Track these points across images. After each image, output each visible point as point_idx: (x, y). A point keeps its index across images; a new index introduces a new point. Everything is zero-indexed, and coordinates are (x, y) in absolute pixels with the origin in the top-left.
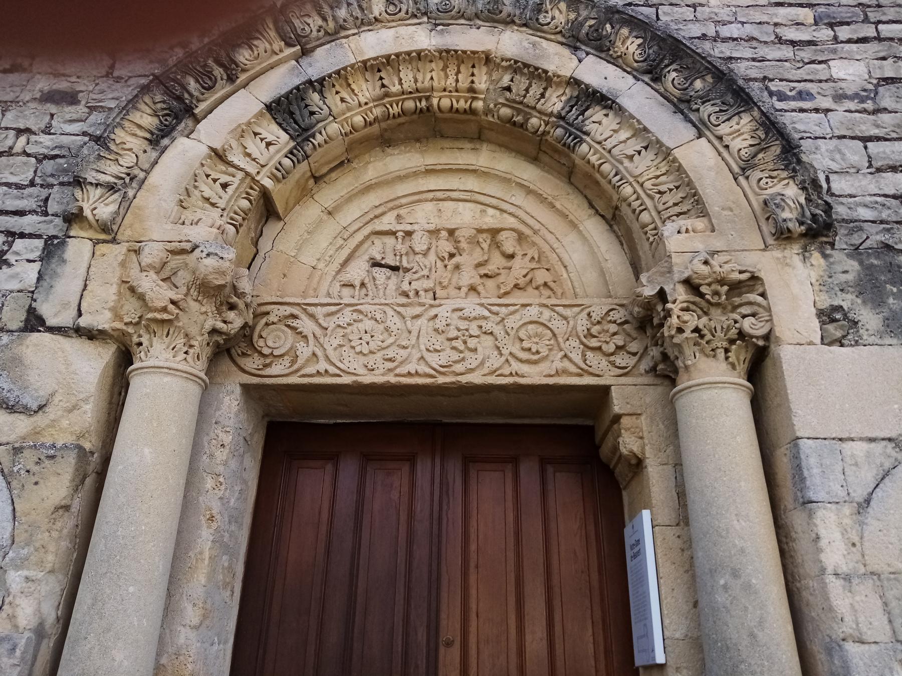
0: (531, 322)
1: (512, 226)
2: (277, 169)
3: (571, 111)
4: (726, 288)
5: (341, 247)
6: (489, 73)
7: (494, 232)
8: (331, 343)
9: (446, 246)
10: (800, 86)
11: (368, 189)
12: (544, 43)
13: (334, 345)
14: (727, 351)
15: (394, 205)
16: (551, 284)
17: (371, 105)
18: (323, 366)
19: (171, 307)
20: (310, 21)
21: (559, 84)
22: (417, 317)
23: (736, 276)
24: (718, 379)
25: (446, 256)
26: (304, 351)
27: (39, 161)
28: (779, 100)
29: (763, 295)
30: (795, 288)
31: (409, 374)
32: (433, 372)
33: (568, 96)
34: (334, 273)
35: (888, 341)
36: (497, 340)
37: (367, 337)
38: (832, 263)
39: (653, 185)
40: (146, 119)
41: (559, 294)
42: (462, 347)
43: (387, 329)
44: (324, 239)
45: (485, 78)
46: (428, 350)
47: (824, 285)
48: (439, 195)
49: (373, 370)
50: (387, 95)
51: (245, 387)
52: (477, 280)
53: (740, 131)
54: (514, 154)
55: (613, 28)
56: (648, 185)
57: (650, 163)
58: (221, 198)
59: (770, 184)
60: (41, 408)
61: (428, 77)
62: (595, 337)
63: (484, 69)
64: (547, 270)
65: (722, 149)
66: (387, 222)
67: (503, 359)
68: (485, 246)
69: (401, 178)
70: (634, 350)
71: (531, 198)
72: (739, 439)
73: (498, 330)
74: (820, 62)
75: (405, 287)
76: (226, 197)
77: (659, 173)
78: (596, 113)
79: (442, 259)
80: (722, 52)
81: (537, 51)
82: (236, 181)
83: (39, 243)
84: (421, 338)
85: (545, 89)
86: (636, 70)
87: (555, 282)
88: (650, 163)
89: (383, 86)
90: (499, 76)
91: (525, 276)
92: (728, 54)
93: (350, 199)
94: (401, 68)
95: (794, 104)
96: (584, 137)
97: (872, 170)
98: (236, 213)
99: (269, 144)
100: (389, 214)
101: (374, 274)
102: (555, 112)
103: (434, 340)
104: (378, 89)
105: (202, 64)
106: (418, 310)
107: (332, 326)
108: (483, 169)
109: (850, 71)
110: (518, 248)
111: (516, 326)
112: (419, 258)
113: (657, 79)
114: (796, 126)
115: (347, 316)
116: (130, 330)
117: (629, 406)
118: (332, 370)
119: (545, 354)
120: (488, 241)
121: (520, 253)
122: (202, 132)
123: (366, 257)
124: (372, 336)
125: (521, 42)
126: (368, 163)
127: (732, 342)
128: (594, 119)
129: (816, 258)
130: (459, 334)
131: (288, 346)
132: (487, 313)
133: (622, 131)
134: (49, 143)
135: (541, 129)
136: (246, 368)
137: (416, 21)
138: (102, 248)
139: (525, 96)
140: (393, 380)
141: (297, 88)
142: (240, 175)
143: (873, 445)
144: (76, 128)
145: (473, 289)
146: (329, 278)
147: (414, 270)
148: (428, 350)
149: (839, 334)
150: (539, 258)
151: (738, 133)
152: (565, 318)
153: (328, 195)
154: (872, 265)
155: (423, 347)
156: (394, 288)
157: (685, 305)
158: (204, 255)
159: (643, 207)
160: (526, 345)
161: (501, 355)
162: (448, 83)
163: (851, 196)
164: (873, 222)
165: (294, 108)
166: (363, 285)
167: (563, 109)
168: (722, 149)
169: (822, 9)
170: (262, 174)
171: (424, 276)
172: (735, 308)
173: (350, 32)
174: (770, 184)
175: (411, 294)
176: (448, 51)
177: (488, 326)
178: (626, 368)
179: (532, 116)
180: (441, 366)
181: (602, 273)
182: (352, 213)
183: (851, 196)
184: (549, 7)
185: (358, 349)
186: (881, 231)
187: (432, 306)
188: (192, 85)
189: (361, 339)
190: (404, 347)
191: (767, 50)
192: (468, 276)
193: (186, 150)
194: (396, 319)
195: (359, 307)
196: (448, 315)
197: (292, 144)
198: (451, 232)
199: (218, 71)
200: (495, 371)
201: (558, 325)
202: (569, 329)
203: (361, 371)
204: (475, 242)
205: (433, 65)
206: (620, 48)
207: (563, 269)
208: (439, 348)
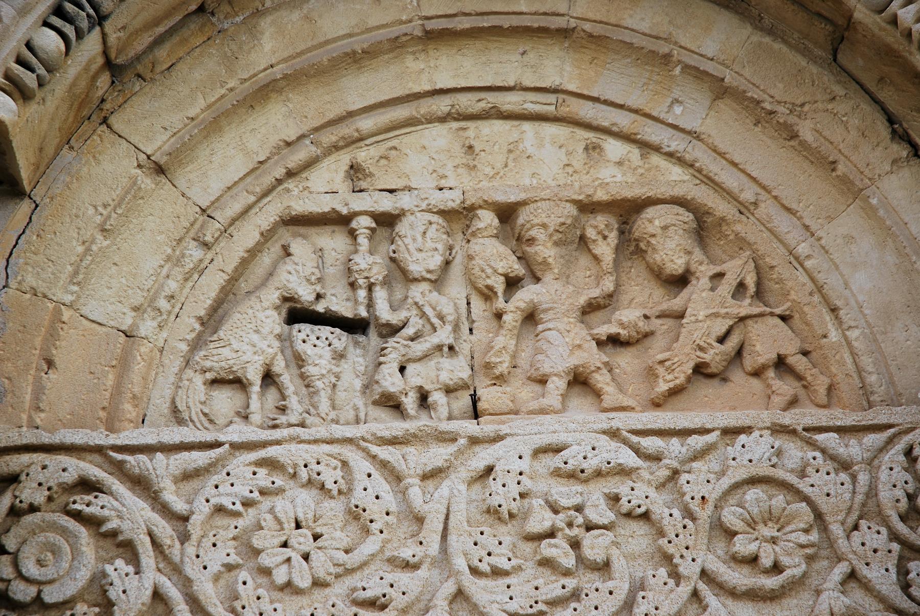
0: (753, 481)
1: (678, 191)
2: (20, 61)
7: (626, 211)
11: (263, 93)
13: (215, 567)
15: (338, 135)
16: (798, 362)
25: (499, 285)
34: (184, 347)
36: (661, 533)
37: (302, 540)
41: (822, 391)
42: (568, 560)
43: (355, 514)
46: (474, 571)
48: (466, 102)
52: (592, 356)
64: (784, 318)
66: (324, 189)
67: (685, 590)
68: (605, 250)
71: (726, 107)
73: (659, 504)
75: (390, 381)
79: (488, 295)
84: (452, 538)
87: (805, 353)
91: (721, 340)
93: (214, 124)
100: (326, 163)
101: (300, 347)
103: (489, 541)
106: (438, 454)
107: (202, 510)
108: (588, 27)
110: (698, 255)
111: (714, 492)
112: (417, 292)
115: (241, 478)
119: (797, 572)
120: (613, 236)
121: (705, 271)
123: (272, 296)
124: (316, 537)
130: (560, 520)
131: (83, 575)
132: (628, 458)
145: (579, 381)
146: (174, 364)
147: (409, 331)
148: (474, 571)
150: (759, 284)
152: (845, 465)
153: (152, 120)
155: (460, 563)
156: (358, 384)
160: (743, 546)
161: (676, 575)
166: (269, 378)
171: (439, 348)
175: (410, 402)
182: (220, 167)
185: (280, 576)
187: (474, 441)
189: (285, 545)
190: (409, 566)
192: (565, 345)
194: (381, 485)
196: (524, 465)
198: (507, 214)
202: (859, 498)
207: (828, 317)
208: (504, 564)
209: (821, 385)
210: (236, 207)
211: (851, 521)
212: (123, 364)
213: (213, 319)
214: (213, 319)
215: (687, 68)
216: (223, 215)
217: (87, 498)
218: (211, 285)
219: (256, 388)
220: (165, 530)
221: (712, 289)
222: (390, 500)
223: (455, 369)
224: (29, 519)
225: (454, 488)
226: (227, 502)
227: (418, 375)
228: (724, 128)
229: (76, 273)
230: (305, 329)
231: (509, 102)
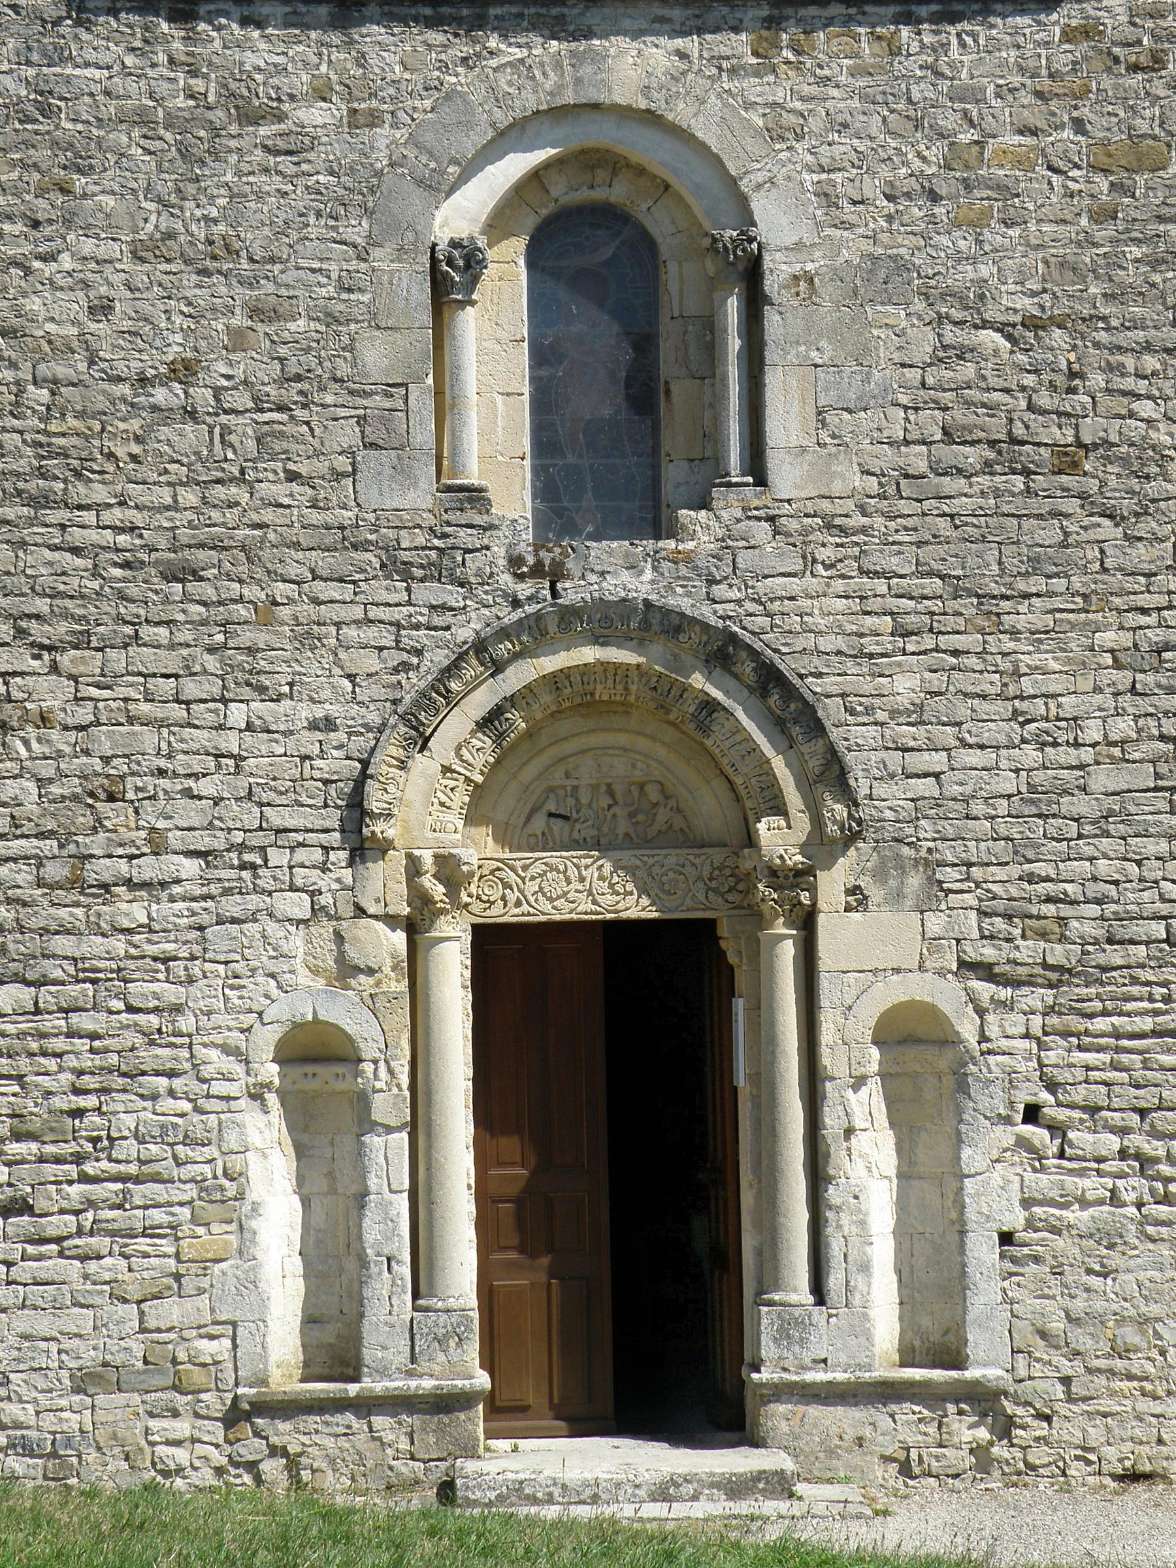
7: (642, 786)
9: (605, 801)
11: (541, 751)
26: (512, 897)
31: (586, 913)
75: (576, 835)
109: (905, 687)
123: (544, 810)
132: (638, 863)
140: (574, 916)
151: (813, 754)
160: (666, 887)
188: (422, 716)
198: (609, 785)
206: (737, 669)
213: (528, 819)
214: (528, 819)
220: (519, 881)
230: (553, 820)
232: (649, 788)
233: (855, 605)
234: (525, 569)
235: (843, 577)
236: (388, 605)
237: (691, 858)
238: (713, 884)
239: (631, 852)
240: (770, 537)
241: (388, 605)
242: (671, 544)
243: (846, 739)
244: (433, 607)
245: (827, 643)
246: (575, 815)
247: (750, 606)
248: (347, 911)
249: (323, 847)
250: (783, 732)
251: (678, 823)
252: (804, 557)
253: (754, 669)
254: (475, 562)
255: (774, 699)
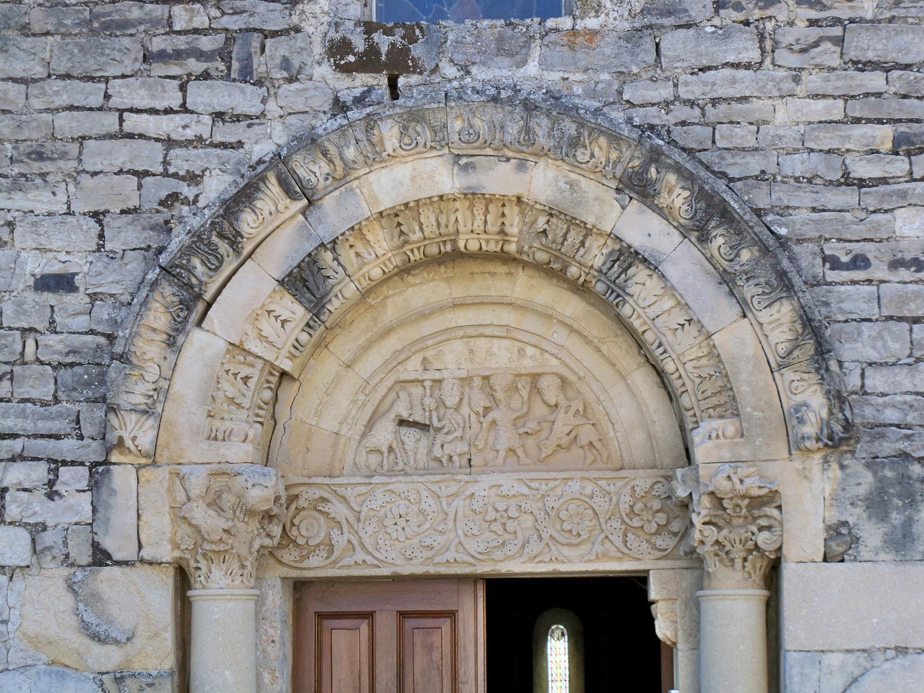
1: (555, 370)
2: (295, 347)
3: (613, 266)
4: (746, 501)
5: (364, 405)
6: (522, 213)
7: (535, 378)
8: (368, 532)
9: (481, 401)
10: (857, 248)
11: (388, 332)
12: (583, 183)
13: (369, 533)
14: (745, 560)
16: (597, 444)
17: (390, 254)
18: (360, 556)
19: (225, 536)
20: (315, 169)
21: (601, 234)
22: (454, 495)
23: (756, 492)
24: (730, 592)
25: (481, 411)
26: (340, 541)
27: (54, 368)
28: (832, 268)
29: (779, 508)
30: (812, 496)
32: (472, 560)
33: (610, 249)
34: (358, 437)
35: (882, 556)
37: (402, 522)
38: (847, 475)
39: (694, 368)
40: (158, 318)
41: (605, 457)
43: (422, 512)
44: (343, 400)
45: (517, 220)
47: (835, 499)
48: (470, 331)
49: (411, 559)
50: (407, 242)
51: (284, 579)
53: (779, 320)
54: (555, 280)
55: (658, 173)
56: (689, 366)
57: (692, 341)
58: (244, 395)
59: (800, 389)
60: (128, 639)
61: (453, 220)
62: (638, 515)
63: (516, 209)
65: (762, 338)
67: (543, 543)
68: (525, 393)
69: (424, 315)
70: (675, 529)
71: (574, 337)
72: (742, 647)
74: (886, 211)
75: (437, 452)
76: (249, 394)
77: (701, 354)
78: (639, 273)
79: (477, 414)
80: (780, 199)
81: (575, 195)
82: (255, 373)
83: (84, 471)
84: (458, 522)
85: (585, 237)
86: (682, 226)
87: (600, 440)
88: (692, 341)
89: (402, 233)
90: (533, 218)
91: (568, 434)
92: (786, 203)
93: (367, 347)
94: (421, 211)
95: (846, 275)
96: (627, 298)
97: (911, 360)
98: (260, 408)
99: (284, 322)
101: (403, 438)
102: (596, 267)
104: (397, 238)
105: (206, 242)
108: (519, 302)
110: (561, 396)
113: (704, 239)
114: (843, 305)
116: (188, 556)
117: (665, 591)
118: (369, 559)
120: (528, 388)
122: (216, 321)
123: (391, 416)
125: (557, 181)
126: (386, 298)
127: (750, 551)
128: (636, 279)
129: (835, 471)
130: (498, 516)
131: (323, 535)
132: (525, 490)
133: (666, 298)
134: (60, 347)
135: (581, 280)
136: (284, 561)
137: (435, 153)
138: (145, 474)
139: (562, 244)
141: (310, 255)
142: (259, 364)
143: (848, 655)
144: (82, 322)
149: (841, 549)
150: (585, 410)
151: (778, 323)
154: (885, 477)
155: (460, 532)
156: (425, 451)
157: (707, 519)
158: (249, 485)
159: (684, 389)
160: (567, 526)
161: (540, 538)
162: (475, 225)
163: (884, 395)
164: (898, 426)
165: (307, 274)
166: (391, 449)
167: (604, 264)
168: (762, 338)
169: (903, 128)
170: (281, 357)
172: (755, 519)
173: (361, 172)
174: (800, 389)
176: (473, 194)
177: (526, 506)
178: (666, 550)
179: (571, 265)
180: (479, 553)
181: (650, 437)
183: (884, 395)
184: (587, 142)
186: (901, 439)
188: (200, 269)
189: (396, 524)
191: (829, 195)
192: (505, 438)
193: (203, 345)
194: (431, 501)
195: (391, 487)
196: (485, 493)
197: (309, 316)
198: (486, 378)
199: (223, 247)
200: (535, 557)
201: (601, 503)
202: (612, 507)
203: (398, 562)
204: (513, 388)
205: (458, 204)
206: (663, 200)
207: (610, 426)
208: (476, 533)
209: (605, 454)
210: (378, 379)
211: (607, 517)
212: (335, 445)
213: (370, 425)
214: (370, 425)
215: (558, 321)
216: (373, 383)
217: (323, 505)
218: (369, 410)
219: (386, 455)
221: (566, 413)
222: (434, 507)
223: (463, 447)
224: (303, 513)
225: (459, 503)
226: (374, 507)
227: (448, 449)
228: (573, 344)
229: (316, 412)
230: (404, 430)
231: (488, 331)
232: (544, 383)
233: (836, 110)
234: (351, 58)
235: (820, 67)
236: (153, 111)
237: (603, 483)
238: (636, 522)
239: (515, 476)
240: (710, 9)
241: (153, 111)
242: (566, 23)
243: (826, 304)
244: (219, 116)
245: (797, 165)
246: (436, 423)
247: (681, 112)
248: (84, 555)
249: (50, 460)
250: (731, 293)
251: (587, 434)
252: (762, 38)
253: (688, 201)
254: (277, 49)
255: (719, 241)
